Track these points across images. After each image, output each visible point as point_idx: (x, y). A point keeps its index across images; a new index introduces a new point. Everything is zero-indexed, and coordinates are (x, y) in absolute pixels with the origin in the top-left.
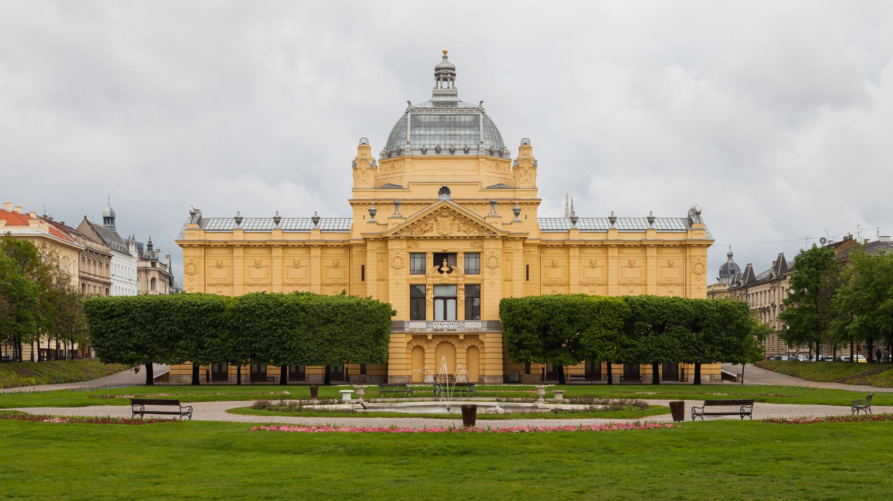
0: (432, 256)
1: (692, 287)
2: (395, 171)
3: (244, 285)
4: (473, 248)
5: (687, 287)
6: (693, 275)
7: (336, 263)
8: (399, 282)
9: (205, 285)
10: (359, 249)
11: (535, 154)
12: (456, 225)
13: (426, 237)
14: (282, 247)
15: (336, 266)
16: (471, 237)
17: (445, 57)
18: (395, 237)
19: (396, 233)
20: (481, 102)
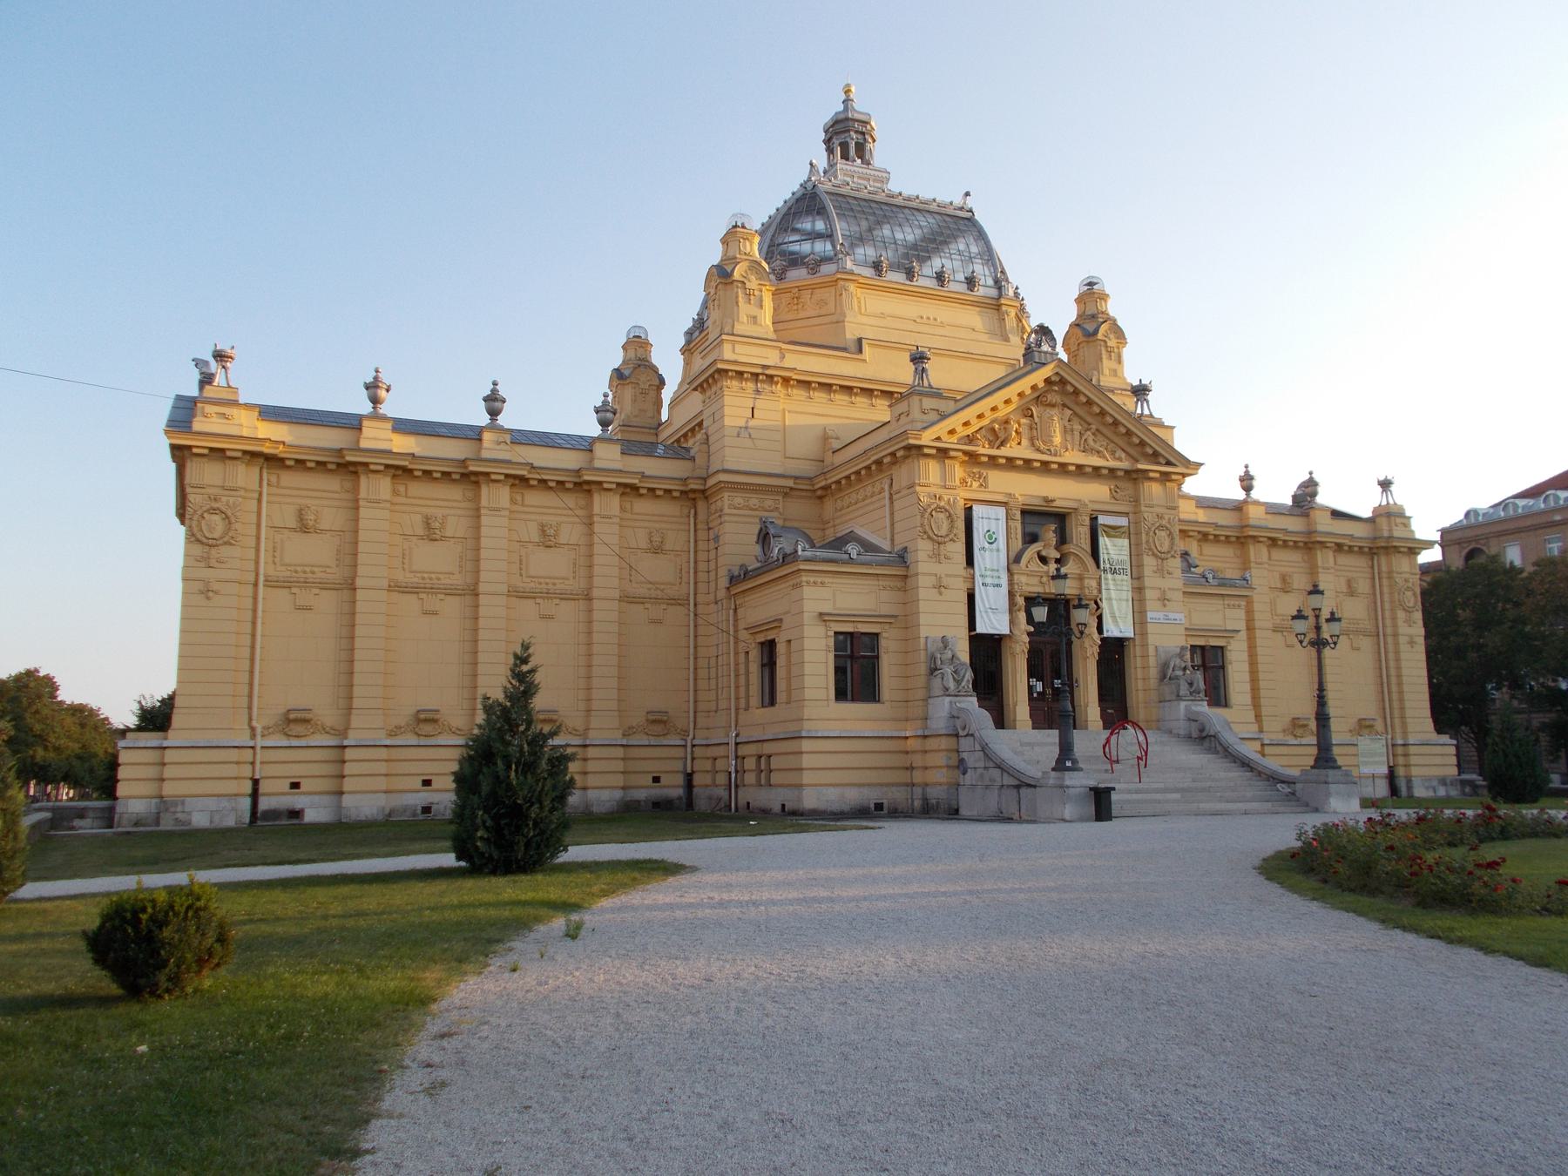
0: (1018, 515)
1: (1402, 640)
2: (800, 316)
3: (390, 589)
4: (1113, 501)
5: (1390, 640)
6: (1401, 615)
7: (657, 539)
8: (945, 582)
9: (256, 585)
10: (739, 500)
11: (1113, 308)
12: (1077, 434)
13: (1010, 463)
14: (511, 481)
15: (657, 550)
16: (1112, 470)
17: (847, 101)
18: (939, 450)
19: (938, 439)
20: (967, 194)
